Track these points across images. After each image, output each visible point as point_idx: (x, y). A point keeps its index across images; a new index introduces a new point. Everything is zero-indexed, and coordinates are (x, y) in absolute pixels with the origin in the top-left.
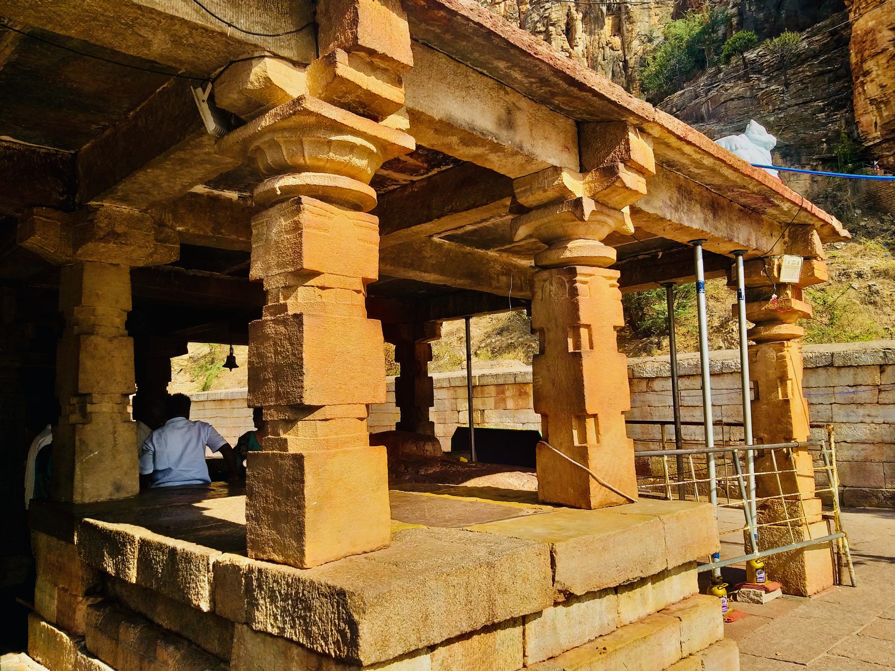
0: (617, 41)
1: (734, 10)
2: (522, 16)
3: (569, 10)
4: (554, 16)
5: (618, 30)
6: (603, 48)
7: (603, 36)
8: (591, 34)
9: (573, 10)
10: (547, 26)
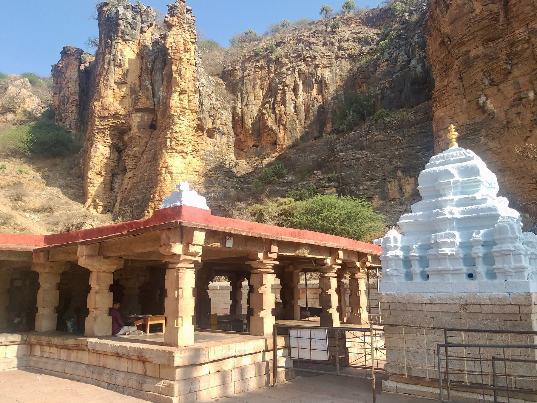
0: (320, 97)
1: (379, 92)
2: (270, 79)
4: (288, 82)
5: (320, 92)
9: (298, 80)
10: (283, 86)
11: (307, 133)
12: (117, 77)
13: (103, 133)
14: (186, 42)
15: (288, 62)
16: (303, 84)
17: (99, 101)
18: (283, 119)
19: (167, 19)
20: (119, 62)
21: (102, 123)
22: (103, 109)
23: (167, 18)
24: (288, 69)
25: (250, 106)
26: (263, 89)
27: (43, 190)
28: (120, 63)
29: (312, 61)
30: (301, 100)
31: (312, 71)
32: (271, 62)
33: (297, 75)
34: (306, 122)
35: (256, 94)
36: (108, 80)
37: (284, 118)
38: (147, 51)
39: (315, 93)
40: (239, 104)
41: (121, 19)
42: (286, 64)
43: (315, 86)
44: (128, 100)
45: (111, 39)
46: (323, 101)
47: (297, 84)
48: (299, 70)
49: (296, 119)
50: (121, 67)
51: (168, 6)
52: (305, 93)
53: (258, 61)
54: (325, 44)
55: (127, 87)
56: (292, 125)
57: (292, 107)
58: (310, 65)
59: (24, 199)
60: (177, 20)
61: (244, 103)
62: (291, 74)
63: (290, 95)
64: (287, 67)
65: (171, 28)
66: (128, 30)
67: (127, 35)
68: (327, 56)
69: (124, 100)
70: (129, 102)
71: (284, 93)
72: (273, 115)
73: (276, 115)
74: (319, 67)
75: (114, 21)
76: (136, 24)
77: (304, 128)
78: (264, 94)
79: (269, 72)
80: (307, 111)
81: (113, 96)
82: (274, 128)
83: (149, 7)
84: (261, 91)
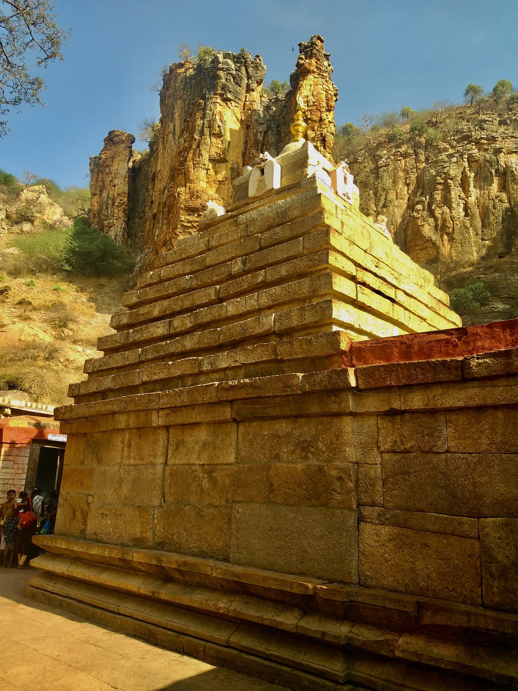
0: (504, 196)
3: (464, 169)
4: (452, 173)
5: (503, 188)
6: (493, 200)
7: (492, 191)
8: (481, 190)
9: (467, 170)
11: (489, 248)
12: (214, 151)
13: (190, 233)
14: (329, 96)
15: (448, 147)
16: (475, 176)
17: (185, 186)
18: (449, 225)
19: (301, 62)
20: (218, 129)
21: (190, 218)
22: (192, 197)
23: (302, 59)
24: (451, 156)
25: (391, 208)
26: (408, 185)
27: (93, 316)
28: (220, 130)
29: (489, 144)
30: (472, 199)
31: (491, 158)
32: (420, 148)
33: (466, 164)
34: (485, 230)
35: (398, 191)
36: (200, 155)
37: (450, 224)
38: (256, 117)
39: (496, 190)
40: (373, 206)
41: (222, 69)
42: (445, 150)
43: (496, 180)
44: (226, 187)
45: (204, 98)
46: (510, 202)
47: (466, 176)
48: (470, 156)
49: (469, 225)
50: (220, 137)
51: (300, 45)
52: (478, 191)
53: (398, 146)
54: (501, 123)
55: (227, 167)
56: (462, 234)
57: (461, 209)
58: (486, 150)
59: (71, 325)
60: (315, 64)
61: (381, 204)
62: (457, 162)
63: (456, 192)
64: (447, 153)
65: (307, 75)
66: (231, 85)
67: (230, 92)
68: (513, 137)
69: (222, 186)
70: (228, 190)
71: (447, 189)
72: (431, 220)
73: (436, 219)
74: (501, 152)
75: (209, 72)
76: (241, 78)
77: (483, 239)
78: (410, 192)
79: (417, 160)
80: (485, 215)
81: (206, 180)
82: (434, 238)
83: (258, 56)
84: (406, 188)
